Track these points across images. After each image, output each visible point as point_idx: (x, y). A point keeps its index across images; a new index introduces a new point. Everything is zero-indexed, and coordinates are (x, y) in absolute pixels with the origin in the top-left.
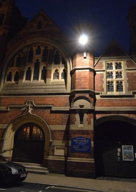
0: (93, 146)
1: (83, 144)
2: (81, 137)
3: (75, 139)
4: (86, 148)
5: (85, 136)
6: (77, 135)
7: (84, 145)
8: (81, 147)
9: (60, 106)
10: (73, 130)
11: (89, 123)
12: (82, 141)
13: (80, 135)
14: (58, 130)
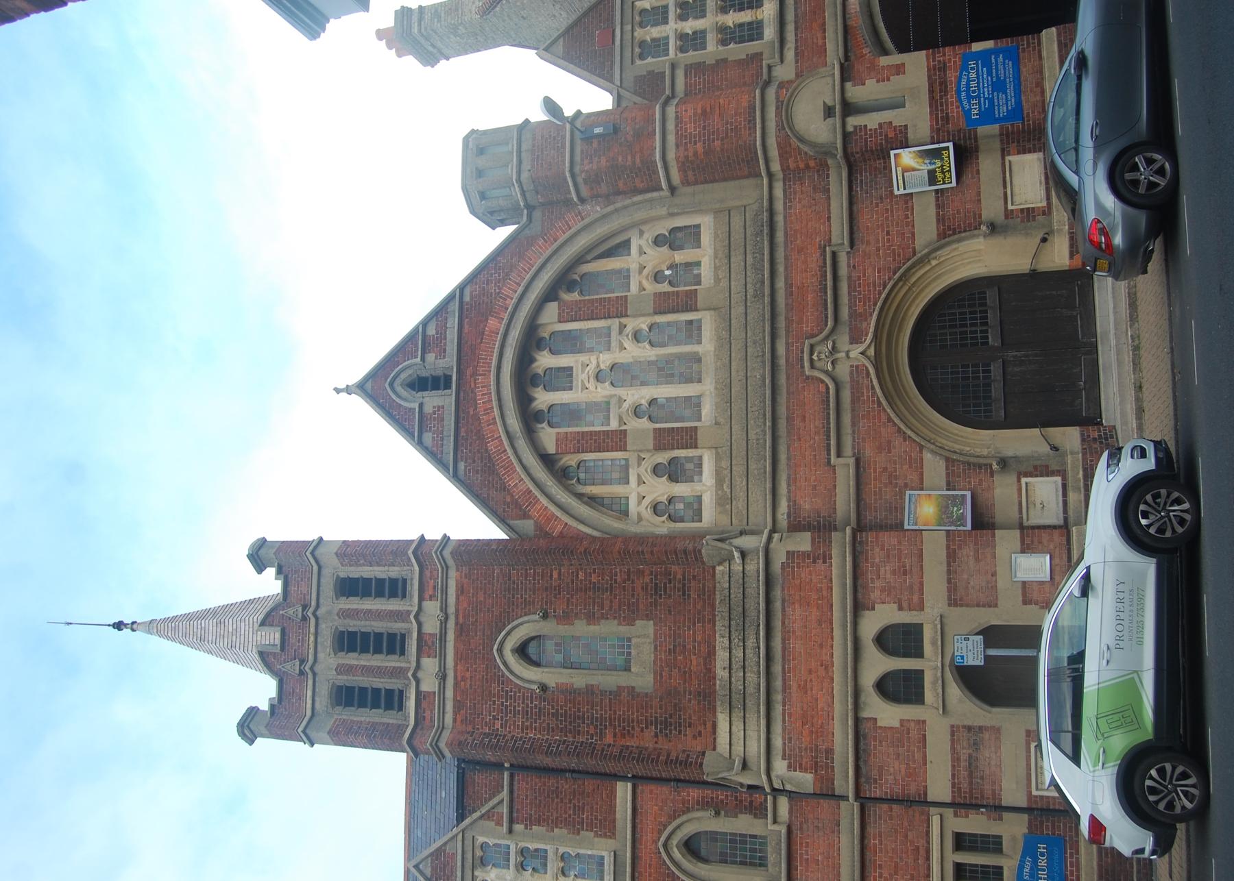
0: (989, 44)
1: (986, 81)
2: (958, 92)
3: (968, 113)
4: (1000, 67)
5: (951, 76)
6: (953, 111)
7: (989, 73)
8: (999, 86)
9: (829, 218)
10: (931, 126)
11: (899, 69)
12: (973, 84)
13: (951, 97)
14: (938, 206)
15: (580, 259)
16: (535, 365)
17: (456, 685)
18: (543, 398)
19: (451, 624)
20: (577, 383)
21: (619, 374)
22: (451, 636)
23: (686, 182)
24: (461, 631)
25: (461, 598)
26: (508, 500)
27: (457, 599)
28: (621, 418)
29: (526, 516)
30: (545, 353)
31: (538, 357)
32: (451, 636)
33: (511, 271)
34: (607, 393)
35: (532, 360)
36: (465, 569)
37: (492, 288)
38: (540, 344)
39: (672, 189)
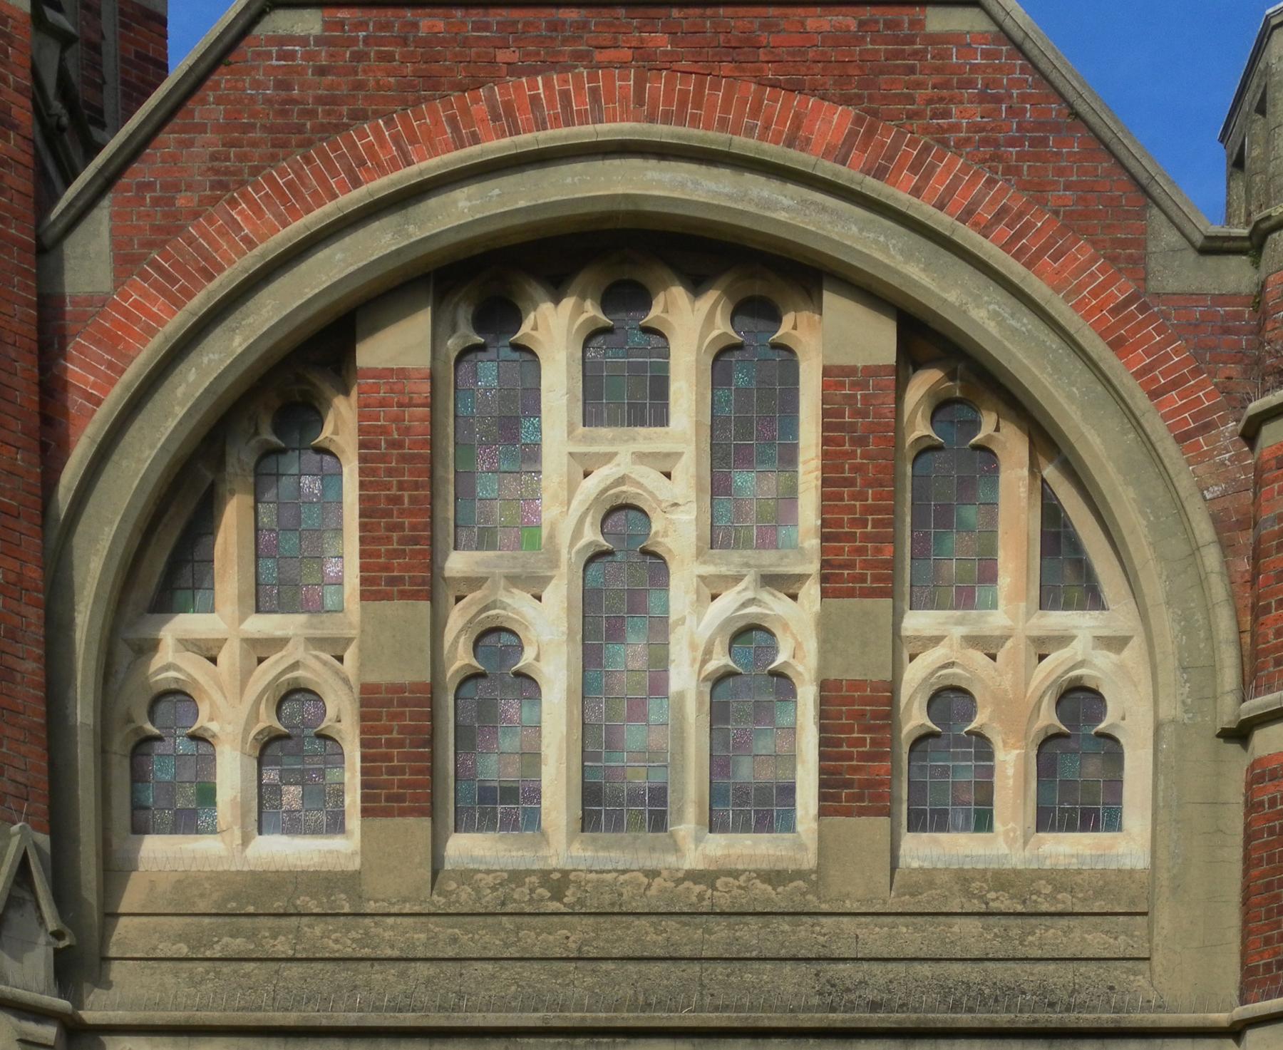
15: (1045, 440)
16: (678, 293)
18: (556, 327)
20: (605, 437)
21: (624, 570)
23: (1258, 775)
26: (183, 200)
28: (475, 582)
29: (125, 263)
30: (722, 327)
31: (711, 297)
33: (1023, 186)
34: (564, 539)
35: (696, 285)
37: (965, 115)
38: (756, 309)
39: (1240, 734)
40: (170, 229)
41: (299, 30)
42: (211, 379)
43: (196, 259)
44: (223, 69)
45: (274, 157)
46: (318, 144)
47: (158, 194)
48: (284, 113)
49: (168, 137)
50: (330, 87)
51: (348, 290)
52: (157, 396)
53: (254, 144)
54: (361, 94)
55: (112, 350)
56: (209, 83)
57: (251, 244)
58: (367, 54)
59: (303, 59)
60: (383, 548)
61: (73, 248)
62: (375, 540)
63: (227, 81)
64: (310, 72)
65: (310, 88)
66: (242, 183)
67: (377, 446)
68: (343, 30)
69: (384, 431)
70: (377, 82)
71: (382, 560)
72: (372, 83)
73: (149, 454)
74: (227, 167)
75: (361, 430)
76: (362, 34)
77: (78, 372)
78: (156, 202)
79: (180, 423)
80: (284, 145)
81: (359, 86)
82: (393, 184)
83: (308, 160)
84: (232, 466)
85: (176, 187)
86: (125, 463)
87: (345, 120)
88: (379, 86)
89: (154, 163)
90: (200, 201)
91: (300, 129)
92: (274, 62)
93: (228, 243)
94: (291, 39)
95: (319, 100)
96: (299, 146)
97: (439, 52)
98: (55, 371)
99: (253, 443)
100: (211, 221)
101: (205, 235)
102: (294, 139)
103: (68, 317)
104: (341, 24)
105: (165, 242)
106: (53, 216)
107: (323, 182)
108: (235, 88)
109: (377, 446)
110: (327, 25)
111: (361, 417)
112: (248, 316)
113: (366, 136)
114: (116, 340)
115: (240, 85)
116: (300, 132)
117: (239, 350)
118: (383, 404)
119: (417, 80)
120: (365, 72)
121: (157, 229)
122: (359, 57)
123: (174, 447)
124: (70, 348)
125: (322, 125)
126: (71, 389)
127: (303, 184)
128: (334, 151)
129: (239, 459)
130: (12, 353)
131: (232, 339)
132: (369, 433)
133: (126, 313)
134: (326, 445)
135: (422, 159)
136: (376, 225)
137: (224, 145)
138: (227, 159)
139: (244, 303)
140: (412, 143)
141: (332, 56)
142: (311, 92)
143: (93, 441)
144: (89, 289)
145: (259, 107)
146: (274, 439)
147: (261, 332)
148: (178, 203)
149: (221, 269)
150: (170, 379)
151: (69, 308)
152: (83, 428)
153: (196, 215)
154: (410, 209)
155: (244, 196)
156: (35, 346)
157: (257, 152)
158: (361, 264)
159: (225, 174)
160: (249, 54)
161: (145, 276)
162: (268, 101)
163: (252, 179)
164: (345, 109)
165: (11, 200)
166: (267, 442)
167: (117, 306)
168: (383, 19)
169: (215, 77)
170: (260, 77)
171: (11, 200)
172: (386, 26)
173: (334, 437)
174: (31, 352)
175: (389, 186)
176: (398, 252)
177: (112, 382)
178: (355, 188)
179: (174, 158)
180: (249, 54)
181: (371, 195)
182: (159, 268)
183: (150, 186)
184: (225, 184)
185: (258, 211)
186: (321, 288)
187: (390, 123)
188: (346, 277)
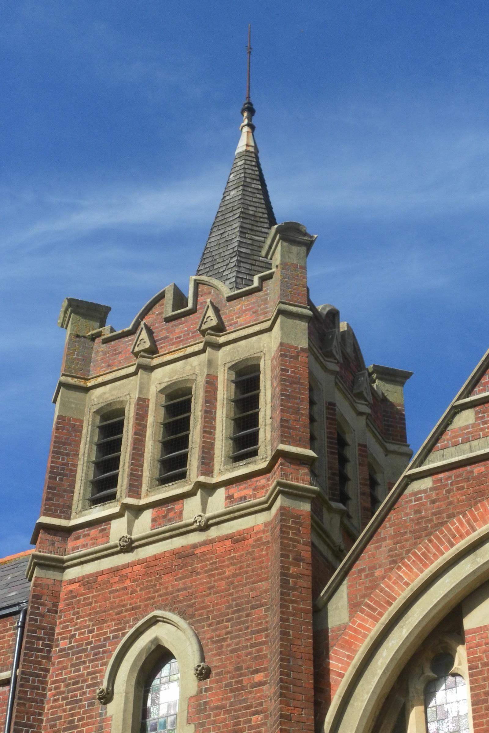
17: (115, 571)
19: (195, 538)
22: (178, 543)
24: (185, 556)
25: (228, 543)
26: (378, 573)
27: (229, 537)
29: (354, 607)
32: (178, 543)
36: (266, 537)
40: (374, 586)
41: (423, 487)
42: (393, 653)
43: (384, 598)
44: (392, 512)
45: (416, 544)
46: (434, 533)
47: (367, 572)
48: (419, 523)
49: (370, 547)
50: (438, 507)
51: (453, 595)
52: (369, 667)
53: (407, 540)
54: (451, 506)
55: (349, 650)
56: (386, 519)
57: (407, 584)
58: (452, 489)
59: (425, 499)
60: (484, 720)
61: (331, 606)
62: (482, 716)
63: (394, 516)
64: (429, 503)
65: (429, 510)
66: (403, 559)
67: (477, 667)
68: (442, 482)
69: (480, 658)
70: (458, 500)
71: (485, 727)
72: (456, 501)
73: (367, 697)
74: (396, 553)
75: (469, 661)
76: (449, 482)
77: (334, 664)
78: (366, 576)
79: (380, 678)
80: (420, 537)
81: (450, 503)
82: (467, 542)
83: (430, 541)
84: (412, 692)
85: (375, 568)
86: (356, 704)
87: (445, 520)
88: (459, 501)
89: (365, 559)
90: (385, 571)
91: (426, 529)
92: (414, 503)
93: (398, 587)
94: (420, 492)
95: (434, 514)
96: (425, 536)
97: (483, 480)
98: (324, 665)
99: (422, 678)
100: (390, 579)
101: (388, 586)
102: (424, 533)
103: (330, 638)
104: (441, 480)
105: (371, 593)
106: (322, 594)
107: (438, 549)
108: (397, 518)
109: (477, 667)
110: (435, 482)
111: (468, 654)
112: (408, 618)
113: (454, 524)
114: (350, 644)
115: (399, 517)
116: (426, 530)
117: (405, 636)
118: (478, 645)
119: (475, 494)
120: (452, 497)
121: (367, 588)
122: (448, 492)
123: (378, 691)
124: (331, 654)
125: (435, 524)
126: (331, 673)
127: (429, 552)
128: (441, 534)
129: (415, 688)
130: (300, 663)
131: (401, 632)
132: (472, 661)
133: (355, 631)
134: (456, 671)
135: (480, 527)
136: (463, 562)
137: (394, 544)
138: (396, 549)
139: (406, 613)
140: (475, 522)
141: (438, 494)
142: (430, 512)
143: (340, 696)
144: (339, 623)
145: (408, 524)
146: (432, 674)
147: (415, 625)
148: (376, 574)
149: (395, 599)
150: (375, 657)
151: (330, 634)
152: (336, 691)
153: (383, 578)
154: (478, 551)
155: (404, 564)
156: (312, 656)
157: (408, 543)
158: (457, 582)
159: (395, 556)
160: (403, 503)
161: (362, 611)
162: (412, 520)
163: (407, 555)
164: (445, 515)
165: (301, 593)
166: (428, 676)
167: (351, 628)
168: (458, 473)
169: (389, 516)
170: (408, 511)
171: (301, 593)
172: (460, 476)
173: (460, 667)
174: (310, 660)
175: (465, 544)
176: (474, 572)
177: (348, 664)
178: (452, 547)
179: (373, 555)
180: (403, 503)
181: (458, 550)
182: (369, 606)
183: (363, 570)
184: (395, 561)
185: (410, 569)
186: (440, 597)
187: (465, 516)
188: (452, 589)
